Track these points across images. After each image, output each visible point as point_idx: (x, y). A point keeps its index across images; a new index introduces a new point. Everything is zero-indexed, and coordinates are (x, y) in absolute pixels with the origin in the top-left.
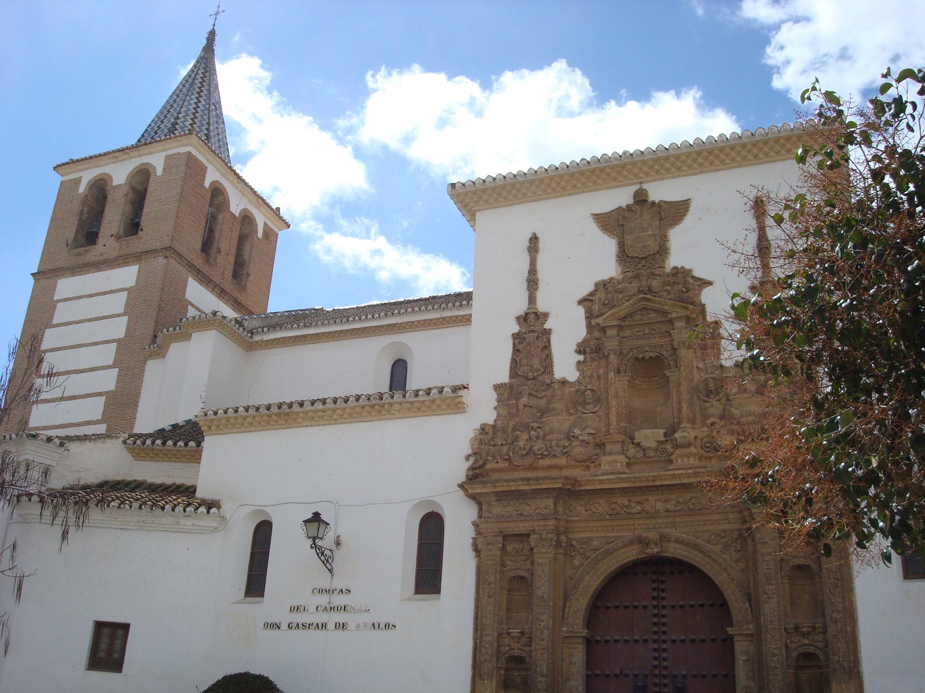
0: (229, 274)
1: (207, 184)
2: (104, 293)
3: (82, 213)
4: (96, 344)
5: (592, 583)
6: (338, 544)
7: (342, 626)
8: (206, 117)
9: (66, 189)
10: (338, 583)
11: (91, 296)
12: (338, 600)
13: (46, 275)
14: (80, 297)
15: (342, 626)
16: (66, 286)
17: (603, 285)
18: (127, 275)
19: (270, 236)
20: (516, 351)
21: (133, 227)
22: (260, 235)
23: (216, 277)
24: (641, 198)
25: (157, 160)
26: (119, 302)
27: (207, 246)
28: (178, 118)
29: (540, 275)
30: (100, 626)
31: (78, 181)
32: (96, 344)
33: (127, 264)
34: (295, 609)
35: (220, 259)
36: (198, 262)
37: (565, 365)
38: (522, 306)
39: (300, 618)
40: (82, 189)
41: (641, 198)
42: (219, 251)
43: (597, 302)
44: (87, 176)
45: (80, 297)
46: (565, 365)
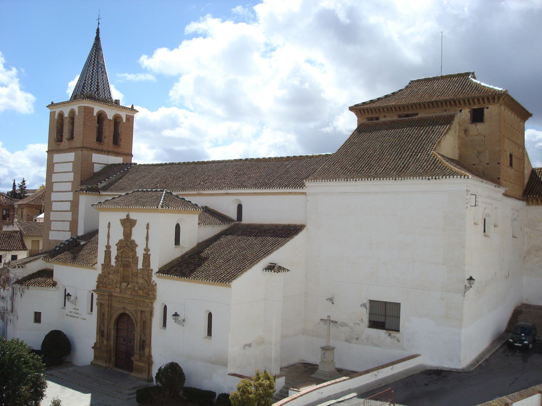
0: (111, 144)
1: (95, 114)
2: (67, 162)
3: (57, 127)
4: (66, 182)
5: (115, 317)
6: (76, 298)
7: (78, 318)
8: (96, 76)
9: (52, 114)
10: (77, 308)
11: (63, 163)
12: (77, 311)
13: (51, 152)
14: (60, 163)
15: (78, 318)
16: (57, 157)
17: (121, 241)
18: (71, 156)
19: (130, 119)
20: (106, 254)
21: (72, 137)
22: (124, 121)
23: (105, 148)
24: (128, 216)
25: (76, 106)
26: (70, 167)
27: (99, 139)
28: (85, 80)
29: (111, 235)
30: (36, 313)
31: (54, 112)
32: (66, 182)
33: (71, 152)
34: (70, 312)
35: (106, 140)
36: (96, 146)
37: (113, 262)
38: (106, 244)
39: (72, 314)
40: (56, 117)
41: (128, 216)
42: (105, 137)
43: (121, 245)
44: (58, 111)
45: (60, 163)
46: (113, 262)
